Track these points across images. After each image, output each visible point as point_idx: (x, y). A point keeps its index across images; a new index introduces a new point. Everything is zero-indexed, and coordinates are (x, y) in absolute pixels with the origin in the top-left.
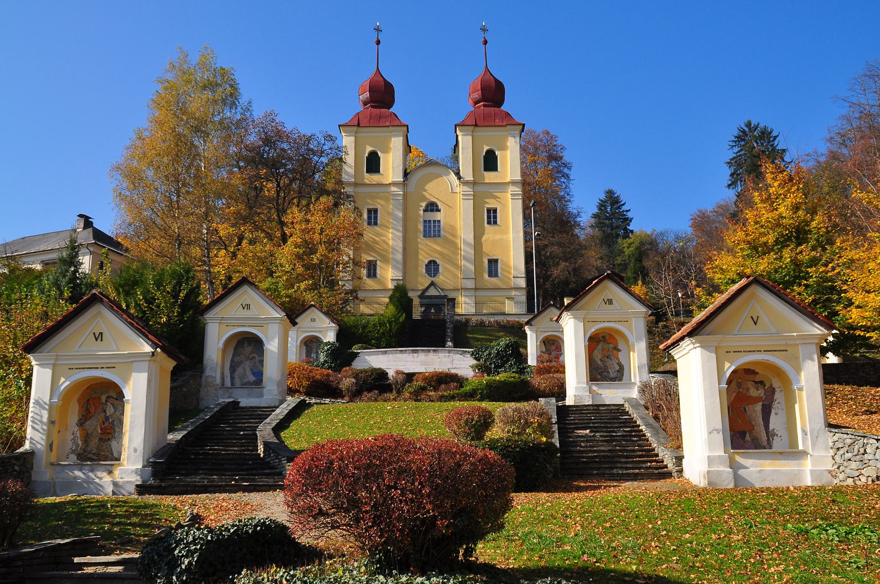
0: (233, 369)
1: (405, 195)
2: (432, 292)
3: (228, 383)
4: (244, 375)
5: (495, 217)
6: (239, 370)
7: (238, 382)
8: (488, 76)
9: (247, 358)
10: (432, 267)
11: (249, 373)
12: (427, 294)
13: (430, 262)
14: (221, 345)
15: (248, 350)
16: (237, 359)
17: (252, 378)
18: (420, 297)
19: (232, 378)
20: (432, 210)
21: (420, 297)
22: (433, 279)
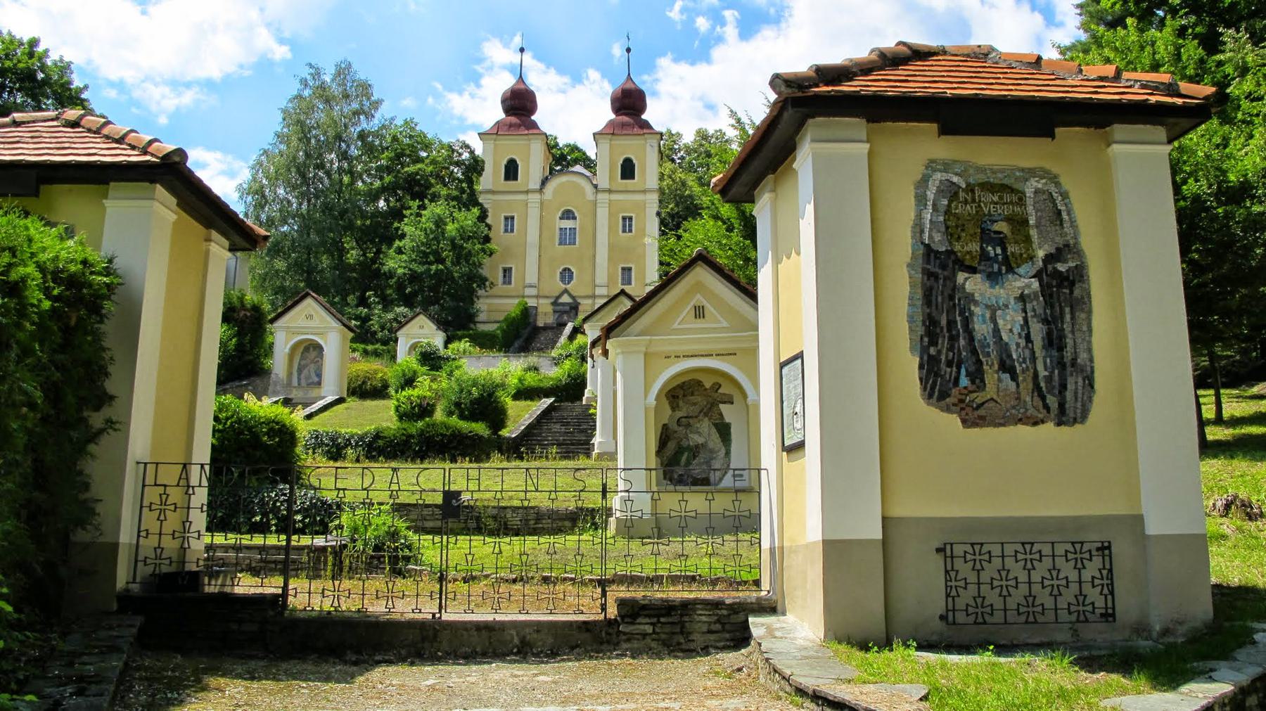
0: (300, 371)
1: (542, 203)
2: (566, 299)
3: (295, 382)
4: (308, 378)
5: (630, 226)
6: (305, 372)
7: (303, 383)
8: (629, 86)
9: (312, 362)
10: (567, 275)
11: (313, 375)
12: (561, 301)
13: (565, 270)
14: (287, 351)
16: (303, 362)
17: (316, 379)
19: (299, 379)
20: (568, 218)
21: (555, 303)
22: (568, 287)
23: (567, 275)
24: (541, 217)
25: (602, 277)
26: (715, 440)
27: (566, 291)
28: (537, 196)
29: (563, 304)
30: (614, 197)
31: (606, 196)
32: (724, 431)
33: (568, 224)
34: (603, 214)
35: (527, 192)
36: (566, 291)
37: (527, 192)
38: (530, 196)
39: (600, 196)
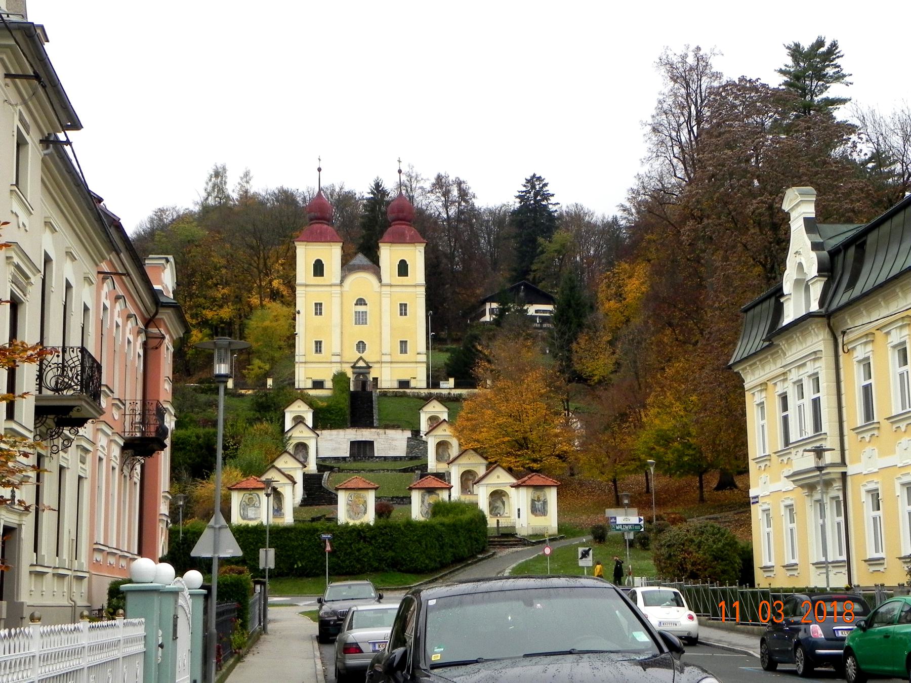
1: (342, 294)
2: (361, 364)
10: (361, 346)
13: (360, 342)
15: (301, 448)
18: (353, 367)
20: (361, 304)
21: (353, 367)
23: (361, 346)
24: (342, 303)
25: (386, 349)
26: (501, 505)
27: (361, 358)
28: (338, 288)
29: (360, 368)
30: (394, 289)
31: (388, 289)
32: (503, 503)
33: (361, 308)
34: (386, 302)
35: (331, 286)
36: (361, 358)
37: (331, 286)
38: (334, 288)
39: (384, 289)
